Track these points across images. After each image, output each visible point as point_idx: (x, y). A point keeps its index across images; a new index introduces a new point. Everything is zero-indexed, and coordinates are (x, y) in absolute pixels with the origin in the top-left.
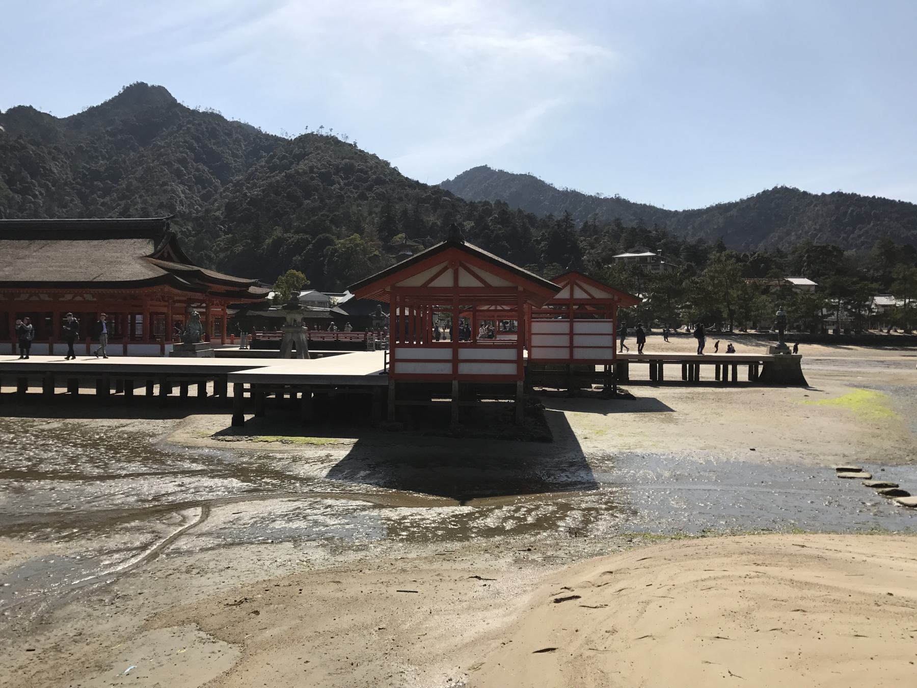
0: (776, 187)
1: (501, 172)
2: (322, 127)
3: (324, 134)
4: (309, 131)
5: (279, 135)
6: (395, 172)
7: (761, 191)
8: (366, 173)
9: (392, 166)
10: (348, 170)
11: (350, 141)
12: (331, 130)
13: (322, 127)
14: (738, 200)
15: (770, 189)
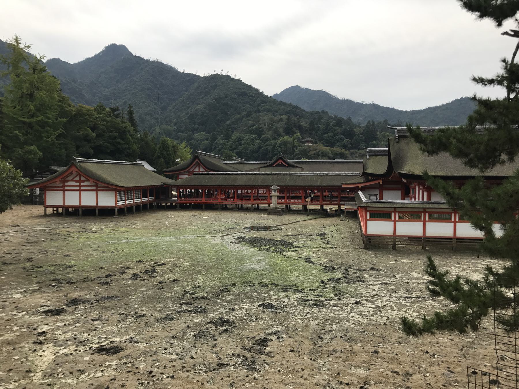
0: (462, 98)
1: (306, 89)
2: (222, 70)
3: (224, 74)
4: (216, 73)
5: (195, 73)
6: (262, 94)
7: (454, 99)
8: (254, 97)
9: (261, 91)
10: (244, 94)
11: (237, 78)
12: (228, 72)
13: (222, 70)
14: (441, 105)
15: (459, 98)
